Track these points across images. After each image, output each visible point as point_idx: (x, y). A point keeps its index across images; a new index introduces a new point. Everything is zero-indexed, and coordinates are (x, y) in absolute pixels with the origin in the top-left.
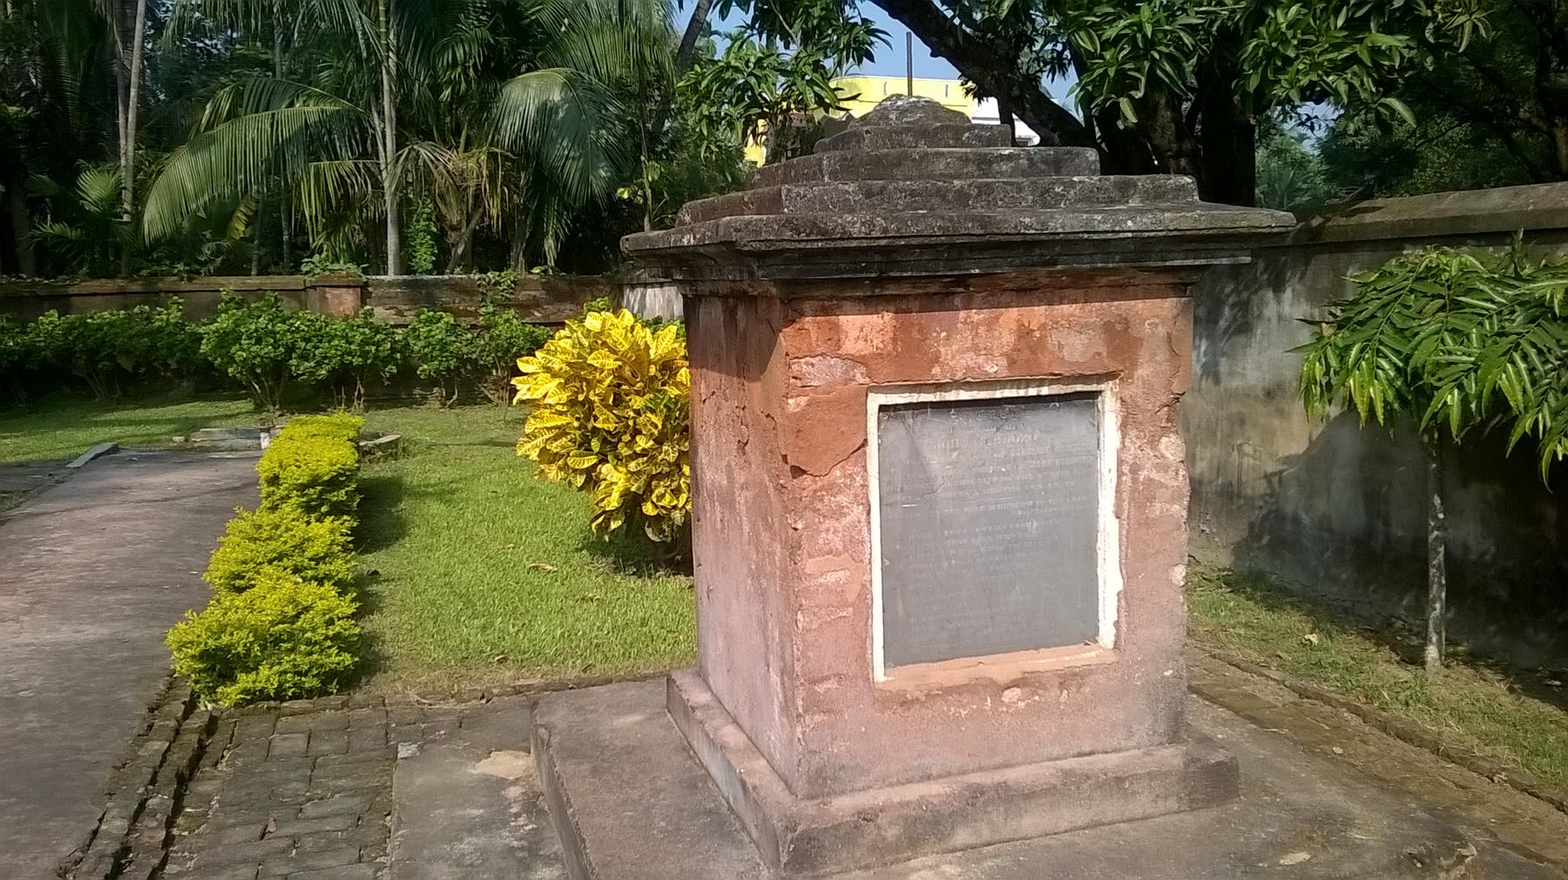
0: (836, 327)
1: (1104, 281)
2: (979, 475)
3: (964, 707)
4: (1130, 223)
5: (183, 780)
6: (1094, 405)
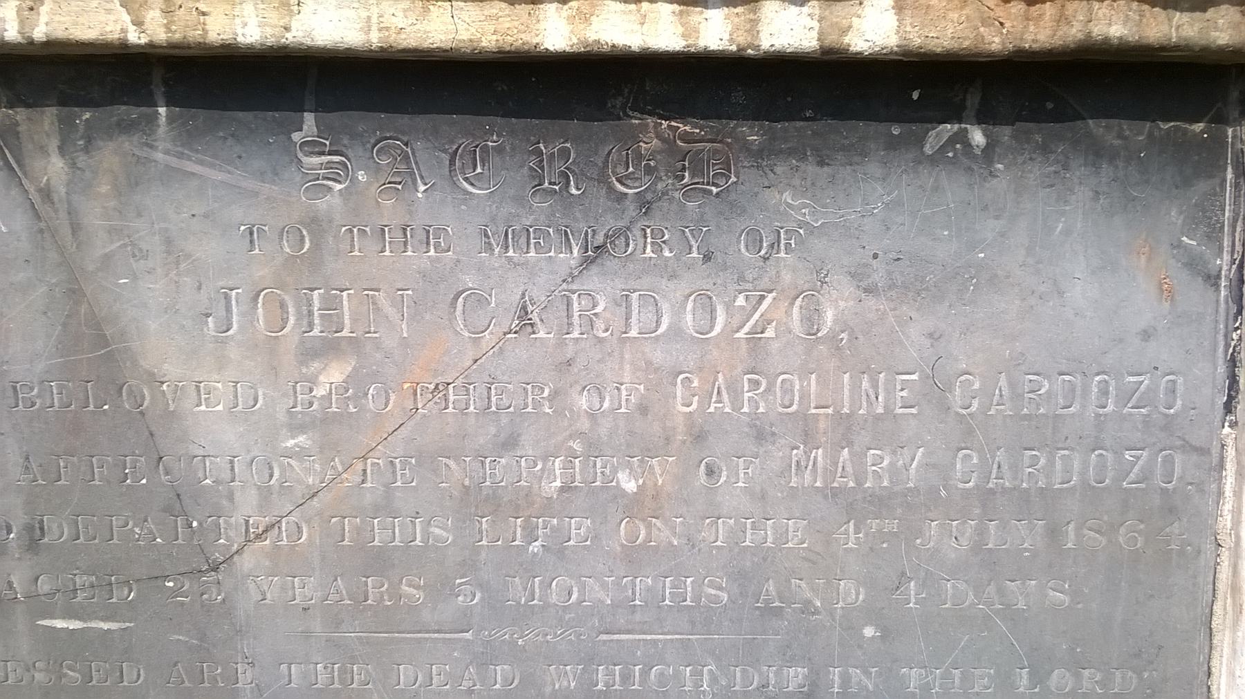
2: (478, 502)
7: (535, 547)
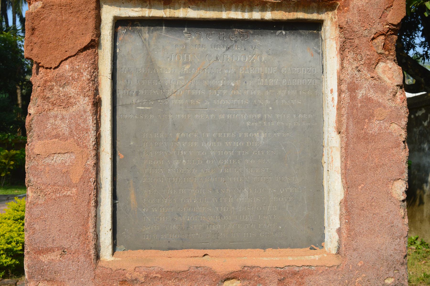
6: (318, 36)
7: (218, 95)
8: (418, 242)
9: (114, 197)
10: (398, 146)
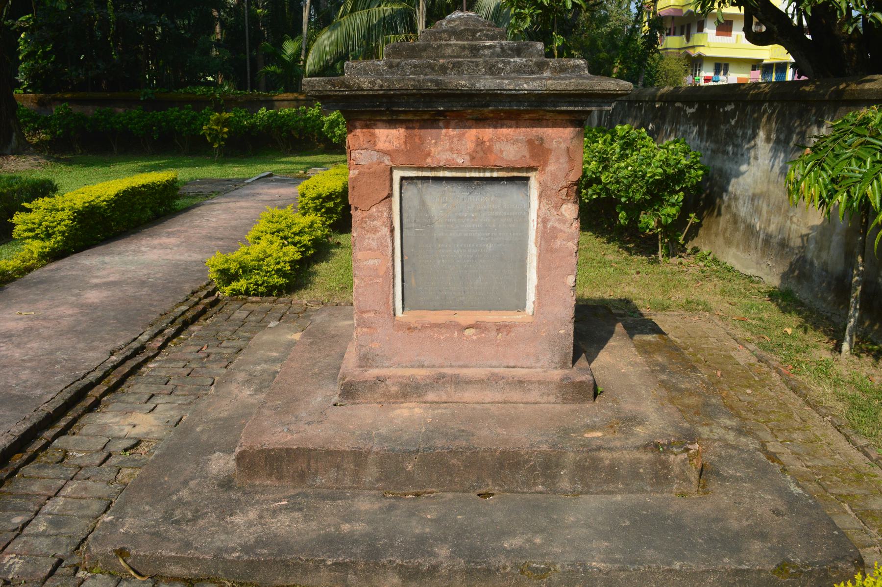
0: (373, 135)
1: (527, 117)
2: (458, 217)
3: (442, 334)
4: (525, 86)
5: (186, 324)
6: (527, 185)
8: (710, 258)
9: (403, 281)
10: (572, 255)
